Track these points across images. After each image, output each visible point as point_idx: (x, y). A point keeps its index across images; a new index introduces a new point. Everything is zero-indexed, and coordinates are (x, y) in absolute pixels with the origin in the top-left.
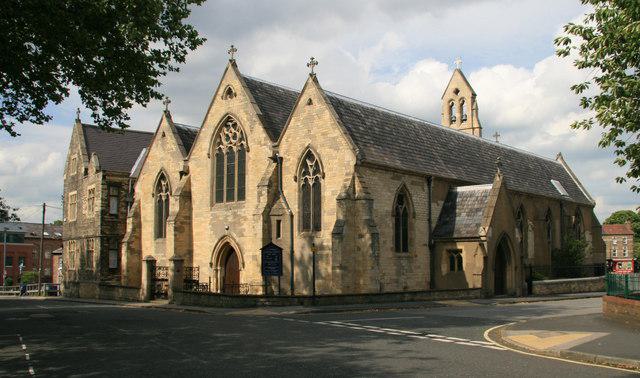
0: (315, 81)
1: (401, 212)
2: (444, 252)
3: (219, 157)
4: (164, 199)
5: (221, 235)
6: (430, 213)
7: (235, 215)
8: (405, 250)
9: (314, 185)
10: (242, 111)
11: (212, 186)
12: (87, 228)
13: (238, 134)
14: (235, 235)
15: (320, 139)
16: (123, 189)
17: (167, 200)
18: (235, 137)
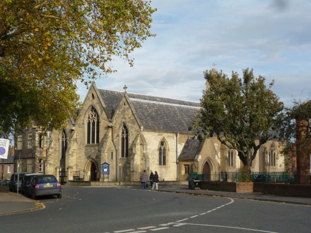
1: (162, 148)
6: (177, 149)
8: (164, 164)
10: (97, 105)
12: (29, 153)
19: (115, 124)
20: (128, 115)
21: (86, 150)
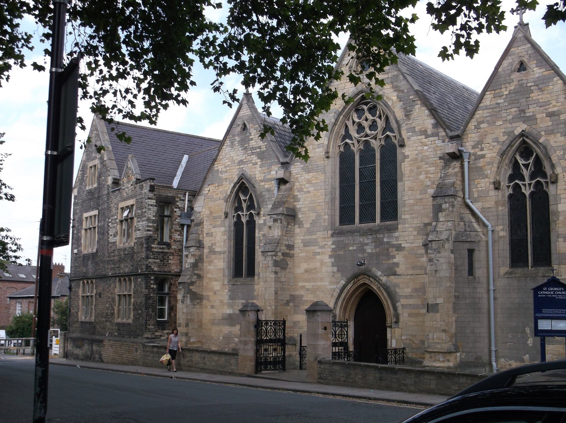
0: (528, 39)
4: (244, 220)
5: (349, 275)
7: (379, 243)
11: (333, 199)
12: (120, 261)
13: (381, 124)
14: (379, 273)
15: (544, 123)
16: (178, 207)
17: (251, 223)
18: (373, 126)
19: (478, 144)
21: (339, 246)
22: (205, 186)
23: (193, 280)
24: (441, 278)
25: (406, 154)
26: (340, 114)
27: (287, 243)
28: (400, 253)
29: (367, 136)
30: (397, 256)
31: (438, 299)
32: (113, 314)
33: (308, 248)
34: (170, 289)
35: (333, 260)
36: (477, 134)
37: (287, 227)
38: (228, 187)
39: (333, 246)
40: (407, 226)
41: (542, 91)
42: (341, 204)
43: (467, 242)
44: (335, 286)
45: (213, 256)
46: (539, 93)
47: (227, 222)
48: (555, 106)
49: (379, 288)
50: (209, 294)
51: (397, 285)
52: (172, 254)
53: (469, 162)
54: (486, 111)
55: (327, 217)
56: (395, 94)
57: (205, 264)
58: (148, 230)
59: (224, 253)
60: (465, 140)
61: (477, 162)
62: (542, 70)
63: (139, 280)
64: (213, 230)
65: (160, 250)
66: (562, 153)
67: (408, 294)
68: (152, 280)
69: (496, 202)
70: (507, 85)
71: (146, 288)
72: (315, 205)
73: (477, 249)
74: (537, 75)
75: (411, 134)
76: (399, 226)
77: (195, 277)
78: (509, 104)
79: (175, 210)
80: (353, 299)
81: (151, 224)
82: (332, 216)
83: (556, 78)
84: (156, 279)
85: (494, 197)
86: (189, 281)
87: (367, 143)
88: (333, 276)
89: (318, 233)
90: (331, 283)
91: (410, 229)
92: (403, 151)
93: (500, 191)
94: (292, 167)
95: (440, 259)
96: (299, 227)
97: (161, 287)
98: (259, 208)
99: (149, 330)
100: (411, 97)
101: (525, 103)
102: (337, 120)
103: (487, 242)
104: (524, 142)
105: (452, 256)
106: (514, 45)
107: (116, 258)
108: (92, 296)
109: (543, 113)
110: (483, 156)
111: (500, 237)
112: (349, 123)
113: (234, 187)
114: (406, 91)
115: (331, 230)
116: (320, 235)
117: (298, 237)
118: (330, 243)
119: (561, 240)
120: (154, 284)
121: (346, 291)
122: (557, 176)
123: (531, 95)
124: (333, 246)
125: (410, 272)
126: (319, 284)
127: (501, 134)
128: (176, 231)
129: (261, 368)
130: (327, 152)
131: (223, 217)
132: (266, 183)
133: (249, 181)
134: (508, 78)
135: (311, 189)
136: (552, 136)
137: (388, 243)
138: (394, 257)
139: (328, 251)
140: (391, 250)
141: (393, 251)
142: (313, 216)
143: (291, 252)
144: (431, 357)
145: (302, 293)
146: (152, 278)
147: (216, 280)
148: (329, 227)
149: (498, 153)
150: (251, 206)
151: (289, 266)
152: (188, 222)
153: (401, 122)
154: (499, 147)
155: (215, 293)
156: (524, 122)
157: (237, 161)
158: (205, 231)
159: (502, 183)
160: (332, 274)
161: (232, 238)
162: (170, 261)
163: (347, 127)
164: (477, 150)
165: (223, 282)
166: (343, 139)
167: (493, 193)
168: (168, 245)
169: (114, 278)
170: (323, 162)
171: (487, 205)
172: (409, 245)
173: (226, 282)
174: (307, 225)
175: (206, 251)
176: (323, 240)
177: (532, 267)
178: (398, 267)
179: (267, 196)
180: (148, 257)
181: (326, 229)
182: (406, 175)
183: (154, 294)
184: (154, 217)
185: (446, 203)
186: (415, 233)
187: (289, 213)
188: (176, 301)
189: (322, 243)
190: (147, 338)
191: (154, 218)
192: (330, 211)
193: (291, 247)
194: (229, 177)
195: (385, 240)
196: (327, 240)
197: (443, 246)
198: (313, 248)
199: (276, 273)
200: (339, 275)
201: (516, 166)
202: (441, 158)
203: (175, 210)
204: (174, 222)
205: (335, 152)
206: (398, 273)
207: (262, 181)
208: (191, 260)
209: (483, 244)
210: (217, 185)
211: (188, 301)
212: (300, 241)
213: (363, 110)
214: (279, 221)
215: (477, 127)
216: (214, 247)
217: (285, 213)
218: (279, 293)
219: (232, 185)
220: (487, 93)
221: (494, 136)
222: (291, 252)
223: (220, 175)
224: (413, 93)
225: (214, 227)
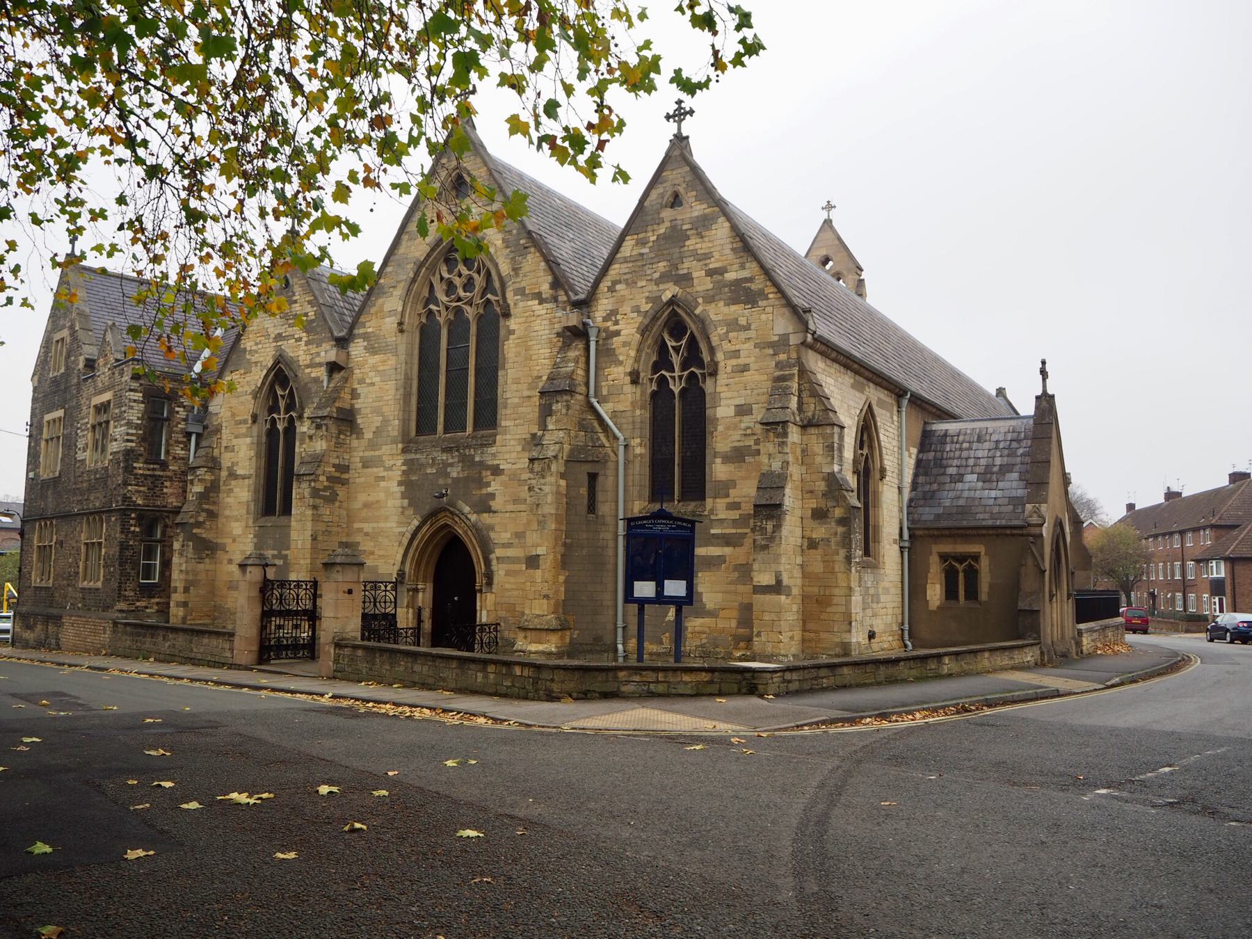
2: (934, 560)
3: (428, 335)
5: (427, 509)
7: (467, 461)
9: (683, 392)
11: (406, 397)
13: (479, 281)
14: (467, 509)
15: (703, 283)
17: (290, 430)
18: (469, 285)
20: (708, 256)
22: (227, 373)
23: (201, 519)
24: (544, 516)
25: (513, 327)
26: (422, 265)
27: (337, 461)
28: (497, 478)
29: (459, 299)
30: (492, 483)
31: (539, 548)
32: (78, 573)
33: (370, 470)
34: (163, 533)
35: (403, 488)
36: (611, 300)
37: (338, 437)
38: (257, 376)
39: (404, 468)
40: (508, 437)
41: (702, 237)
42: (418, 403)
43: (587, 461)
44: (404, 530)
45: (233, 483)
46: (698, 240)
47: (255, 429)
48: (717, 261)
49: (466, 532)
50: (224, 541)
51: (491, 528)
52: (171, 479)
53: (597, 342)
54: (626, 265)
55: (397, 422)
56: (500, 236)
57: (221, 495)
58: (128, 441)
59: (249, 477)
60: (594, 309)
61: (609, 341)
62: (705, 206)
63: (113, 519)
64: (235, 442)
65: (148, 473)
66: (724, 331)
67: (506, 541)
68: (133, 519)
69: (632, 403)
70: (655, 227)
71: (122, 532)
72: (381, 403)
73: (601, 472)
74: (696, 214)
75: (519, 297)
76: (498, 437)
77: (204, 514)
78: (656, 256)
79: (177, 409)
80: (430, 549)
81: (134, 431)
82: (405, 422)
83: (722, 219)
84: (140, 519)
85: (629, 395)
86: (192, 521)
87: (459, 311)
88: (402, 513)
89: (384, 447)
90: (400, 523)
91: (513, 442)
92: (507, 323)
93: (639, 387)
94: (352, 345)
95: (543, 487)
96: (357, 438)
97: (149, 529)
98: (303, 409)
99: (126, 599)
100: (522, 242)
101: (678, 255)
102: (417, 274)
103: (617, 462)
104: (674, 313)
105: (563, 483)
106: (669, 167)
107: (84, 485)
108: (51, 546)
109: (702, 270)
110: (617, 333)
111: (635, 456)
112: (436, 280)
113: (266, 376)
114: (515, 231)
115: (403, 442)
116: (386, 450)
117: (355, 454)
118: (399, 463)
119: (718, 460)
120: (135, 526)
121: (419, 536)
122: (716, 364)
123: (687, 243)
124: (404, 468)
125: (511, 507)
126: (382, 525)
127: (644, 300)
128: (178, 442)
129: (270, 656)
130: (400, 324)
131: (250, 422)
132: (314, 370)
133: (287, 364)
134: (656, 216)
135: (377, 379)
136: (713, 305)
137: (481, 463)
138: (488, 484)
139: (397, 475)
140: (484, 473)
141: (487, 474)
142: (377, 421)
143: (345, 476)
144: (525, 637)
145: (358, 539)
146: (133, 515)
147: (237, 520)
148: (400, 438)
149: (638, 328)
150: (290, 407)
151: (338, 498)
152: (200, 430)
153: (506, 279)
154: (640, 319)
155: (234, 541)
156: (676, 283)
157: (273, 336)
158: (224, 444)
159: (642, 375)
160: (400, 510)
161: (263, 455)
162: (165, 490)
163: (432, 286)
164: (609, 323)
165: (247, 522)
166: (426, 305)
167: (629, 388)
168: (164, 466)
169: (80, 517)
170: (394, 339)
171: (620, 407)
172: (509, 466)
173: (250, 522)
174: (368, 435)
175: (224, 474)
176: (391, 457)
177: (679, 501)
178: (494, 499)
179: (313, 390)
180: (126, 484)
181: (394, 442)
182: (511, 361)
183: (135, 541)
184: (138, 419)
185: (557, 402)
186: (519, 448)
187: (341, 417)
188: (172, 550)
189: (388, 463)
190: (121, 611)
191: (139, 422)
192: (401, 413)
193: (344, 468)
194: (261, 359)
195: (477, 459)
196: (396, 457)
197: (549, 467)
198: (375, 470)
199: (315, 507)
200: (410, 512)
201: (663, 348)
202: (558, 335)
203: (177, 409)
204: (175, 429)
205: (412, 322)
206: (493, 509)
207: (308, 366)
208: (198, 488)
209: (611, 465)
210: (242, 371)
211: (190, 551)
212: (358, 460)
213: (456, 260)
214: (324, 428)
215: (611, 289)
216: (235, 468)
217: (335, 415)
218: (320, 538)
219: (265, 372)
220: (628, 238)
221: (634, 303)
222: (345, 476)
223: (248, 357)
224: (525, 235)
225: (236, 437)
